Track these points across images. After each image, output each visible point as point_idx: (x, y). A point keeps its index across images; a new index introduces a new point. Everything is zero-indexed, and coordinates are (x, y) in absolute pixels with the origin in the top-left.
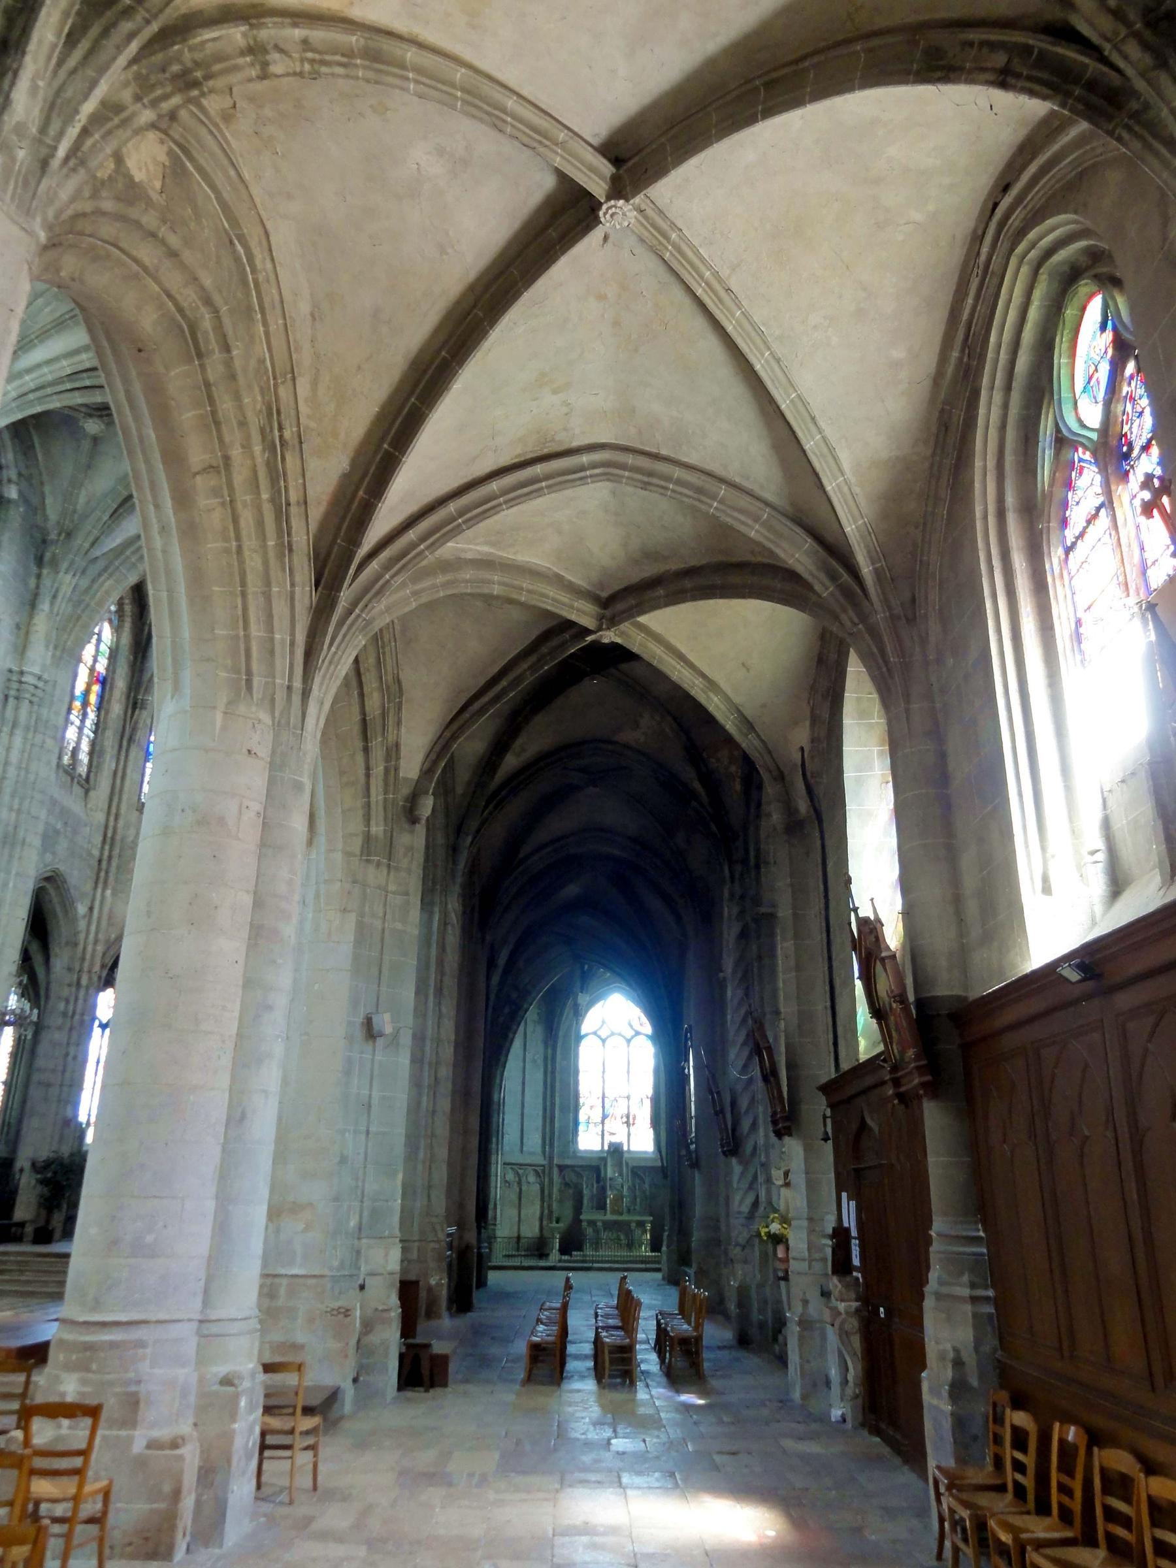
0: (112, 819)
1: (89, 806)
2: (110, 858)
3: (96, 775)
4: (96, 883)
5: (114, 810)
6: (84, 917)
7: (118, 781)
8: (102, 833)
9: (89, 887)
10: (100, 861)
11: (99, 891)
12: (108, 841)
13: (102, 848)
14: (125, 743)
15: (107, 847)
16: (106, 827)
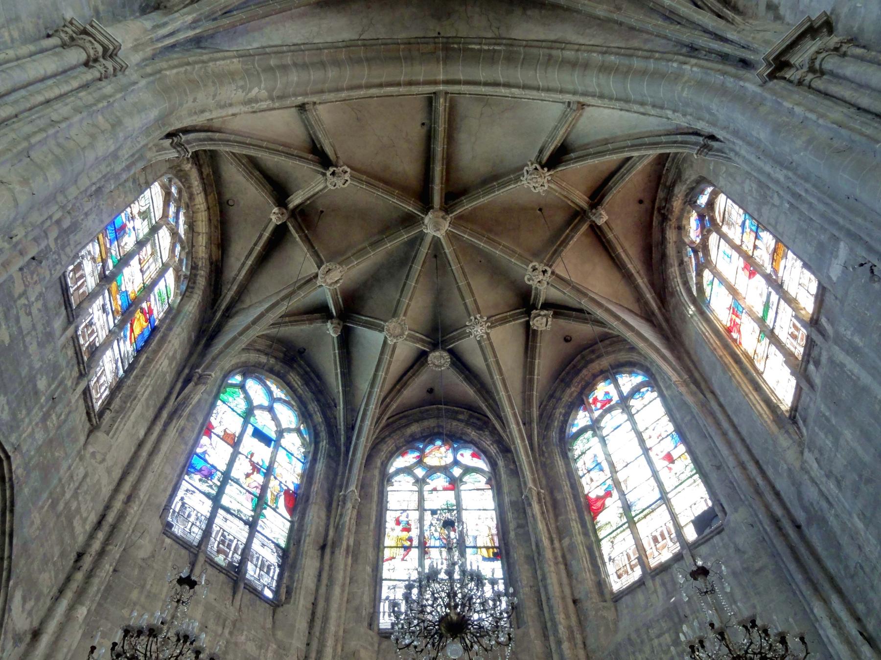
0: (121, 497)
1: (91, 449)
2: (102, 553)
3: (114, 420)
4: (61, 591)
5: (127, 487)
6: (18, 639)
7: (144, 454)
8: (100, 508)
9: (48, 581)
10: (80, 556)
11: (64, 604)
12: (106, 527)
13: (91, 536)
14: (165, 415)
15: (101, 536)
16: (108, 507)
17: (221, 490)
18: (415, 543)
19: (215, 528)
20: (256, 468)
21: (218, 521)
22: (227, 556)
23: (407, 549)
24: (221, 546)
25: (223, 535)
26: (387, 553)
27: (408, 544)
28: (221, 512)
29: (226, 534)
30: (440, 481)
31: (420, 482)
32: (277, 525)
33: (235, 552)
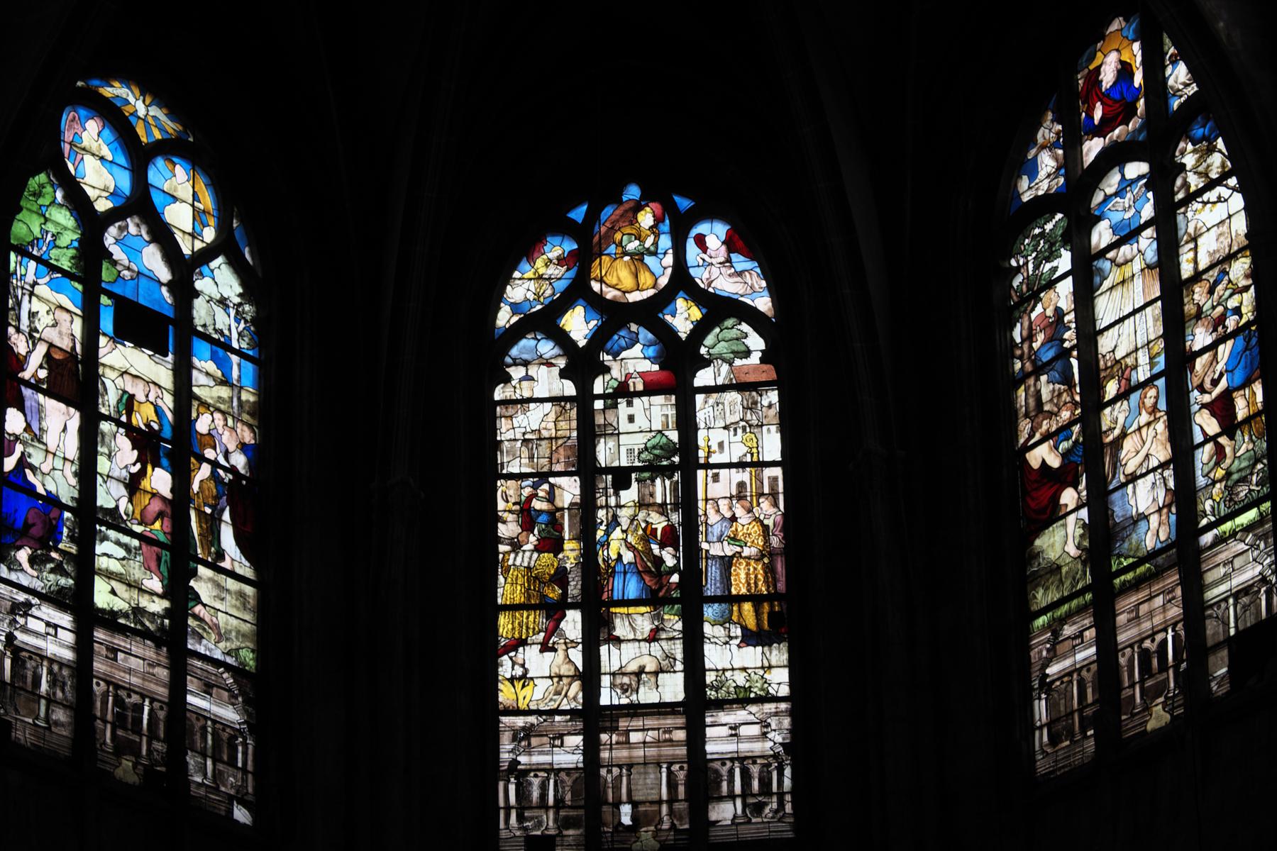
17: (85, 568)
18: (574, 589)
19: (99, 688)
20: (146, 444)
21: (99, 666)
22: (137, 754)
23: (555, 612)
24: (120, 733)
25: (118, 702)
26: (505, 625)
27: (554, 593)
28: (99, 634)
29: (122, 693)
30: (636, 360)
31: (583, 365)
32: (224, 607)
33: (152, 736)
